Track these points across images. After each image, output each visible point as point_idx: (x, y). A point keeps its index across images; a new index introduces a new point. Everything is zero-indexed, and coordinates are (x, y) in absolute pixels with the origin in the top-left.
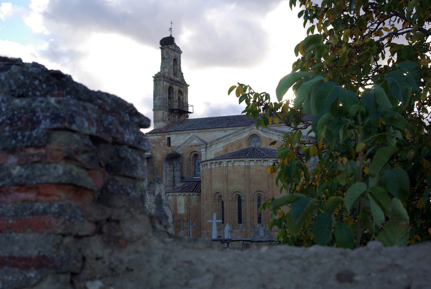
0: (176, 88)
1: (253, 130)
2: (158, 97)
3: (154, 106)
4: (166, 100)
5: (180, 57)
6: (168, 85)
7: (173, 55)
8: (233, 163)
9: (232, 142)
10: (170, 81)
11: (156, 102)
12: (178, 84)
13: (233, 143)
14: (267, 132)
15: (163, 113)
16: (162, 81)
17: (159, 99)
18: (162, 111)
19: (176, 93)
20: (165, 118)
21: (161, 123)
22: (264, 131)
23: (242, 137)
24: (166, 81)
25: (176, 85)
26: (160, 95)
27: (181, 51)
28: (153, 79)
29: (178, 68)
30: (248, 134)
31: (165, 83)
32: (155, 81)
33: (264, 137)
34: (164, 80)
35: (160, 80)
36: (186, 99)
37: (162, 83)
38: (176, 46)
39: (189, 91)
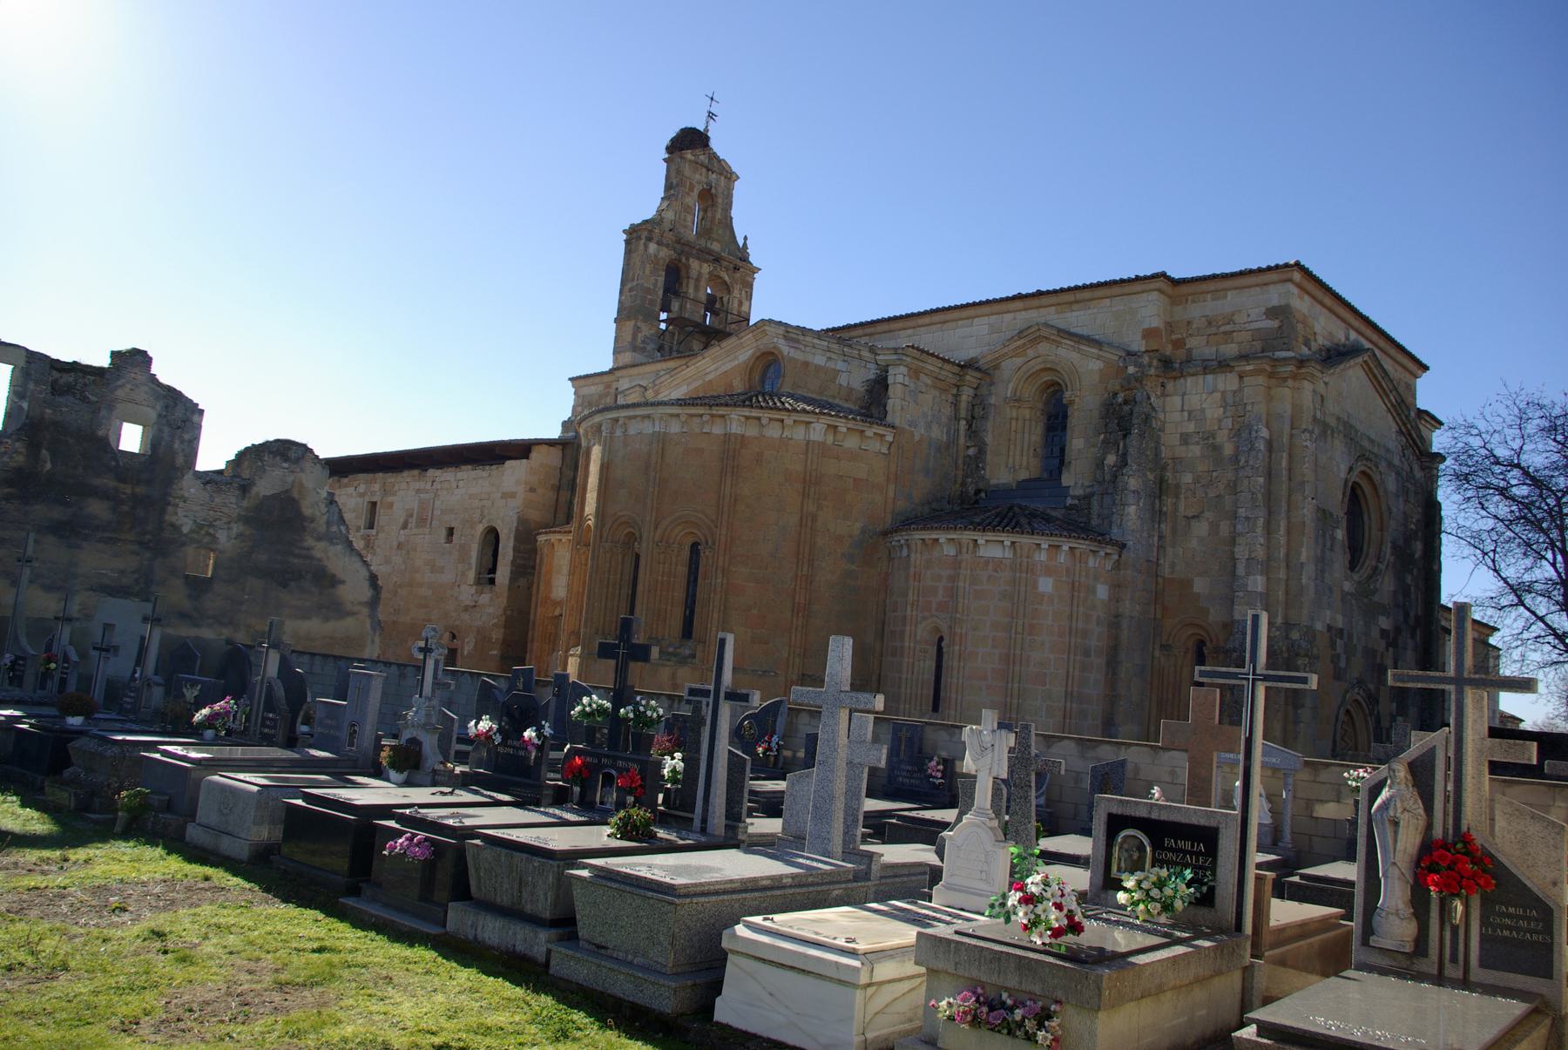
0: (698, 267)
6: (665, 253)
7: (699, 178)
14: (798, 341)
15: (637, 329)
18: (632, 323)
22: (792, 340)
24: (658, 243)
27: (732, 173)
29: (718, 216)
31: (652, 247)
32: (627, 242)
34: (649, 239)
35: (639, 238)
36: (741, 304)
37: (642, 247)
39: (756, 285)
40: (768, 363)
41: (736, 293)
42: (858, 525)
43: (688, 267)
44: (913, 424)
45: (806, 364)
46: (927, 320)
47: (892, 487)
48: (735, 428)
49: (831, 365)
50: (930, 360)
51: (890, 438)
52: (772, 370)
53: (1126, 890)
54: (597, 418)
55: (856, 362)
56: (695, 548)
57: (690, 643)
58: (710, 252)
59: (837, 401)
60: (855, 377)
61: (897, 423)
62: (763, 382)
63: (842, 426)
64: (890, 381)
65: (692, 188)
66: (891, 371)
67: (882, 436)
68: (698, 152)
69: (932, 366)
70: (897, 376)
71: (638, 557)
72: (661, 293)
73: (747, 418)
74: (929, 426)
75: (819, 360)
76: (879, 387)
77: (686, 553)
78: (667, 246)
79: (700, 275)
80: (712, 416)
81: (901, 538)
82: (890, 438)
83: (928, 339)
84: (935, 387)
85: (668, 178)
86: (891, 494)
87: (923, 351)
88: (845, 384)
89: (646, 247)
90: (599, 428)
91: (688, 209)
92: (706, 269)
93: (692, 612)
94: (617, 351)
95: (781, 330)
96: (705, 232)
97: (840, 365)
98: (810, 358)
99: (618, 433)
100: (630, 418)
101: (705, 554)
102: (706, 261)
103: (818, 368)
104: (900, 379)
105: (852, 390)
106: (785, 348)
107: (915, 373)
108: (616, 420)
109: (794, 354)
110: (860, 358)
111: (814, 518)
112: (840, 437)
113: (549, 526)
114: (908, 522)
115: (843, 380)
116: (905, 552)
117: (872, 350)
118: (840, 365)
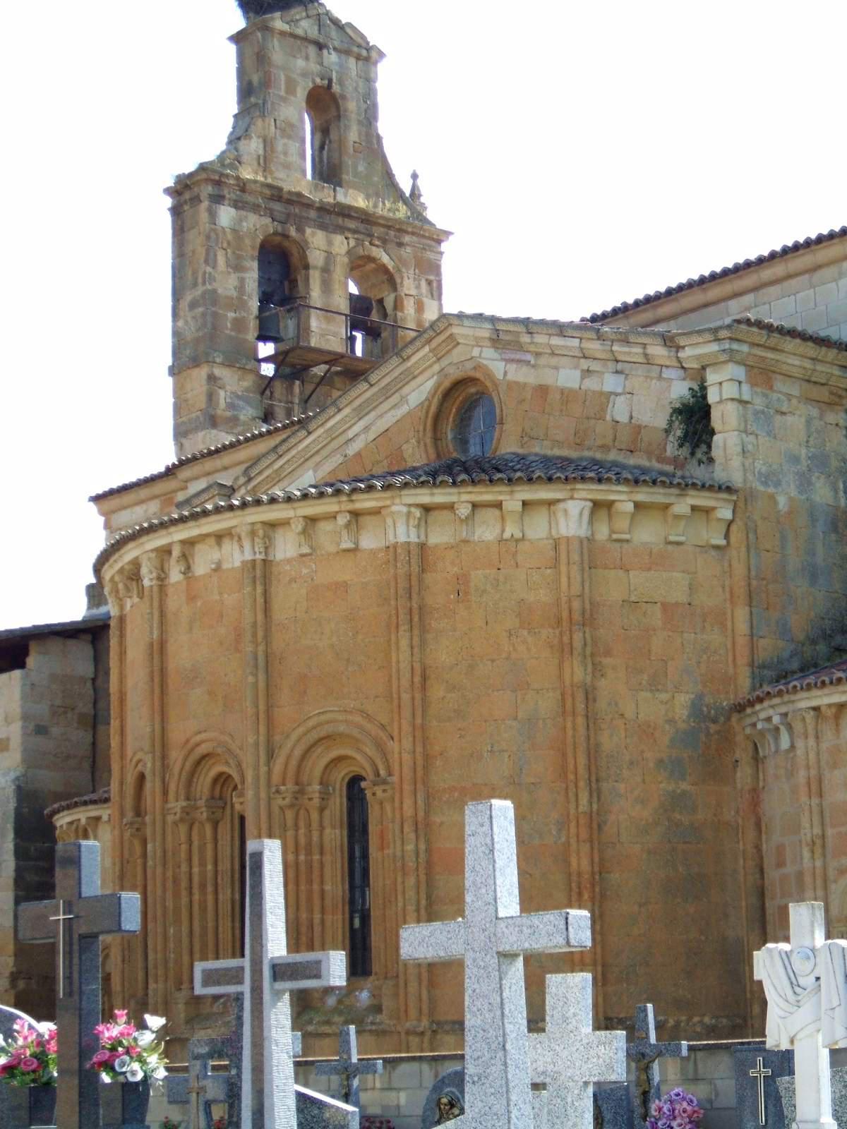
0: (322, 246)
1: (457, 355)
2: (188, 297)
3: (177, 352)
4: (240, 304)
5: (369, 80)
6: (257, 225)
8: (185, 558)
9: (352, 450)
10: (277, 207)
11: (180, 323)
12: (352, 224)
13: (359, 455)
14: (520, 347)
16: (205, 204)
17: (193, 305)
18: (203, 372)
19: (326, 270)
20: (231, 406)
21: (201, 434)
23: (404, 409)
24: (236, 205)
25: (323, 227)
26: (195, 285)
27: (369, 49)
28: (168, 202)
29: (353, 135)
30: (430, 384)
31: (226, 215)
32: (176, 211)
33: (512, 386)
34: (218, 199)
35: (196, 200)
36: (420, 307)
37: (204, 216)
38: (335, 22)
40: (465, 401)
41: (409, 285)
42: (683, 701)
43: (303, 248)
44: (769, 478)
45: (543, 390)
46: (778, 269)
47: (742, 614)
48: (404, 533)
49: (591, 384)
50: (791, 344)
51: (726, 514)
52: (479, 413)
53: (267, 360)
54: (130, 553)
55: (641, 371)
56: (354, 783)
57: (370, 982)
58: (345, 212)
59: (612, 456)
60: (647, 401)
61: (737, 479)
62: (463, 442)
63: (623, 498)
64: (712, 397)
65: (291, 89)
66: (712, 377)
67: (707, 511)
68: (297, 12)
69: (794, 357)
70: (724, 388)
71: (242, 819)
72: (254, 304)
73: (427, 509)
74: (805, 483)
75: (568, 377)
76: (695, 419)
77: (338, 803)
78: (255, 208)
79: (329, 256)
80: (356, 514)
81: (771, 712)
82: (726, 514)
83: (781, 307)
84: (809, 400)
85: (242, 72)
86: (742, 627)
87: (769, 328)
88: (623, 418)
89: (213, 215)
90: (133, 575)
91: (290, 131)
92: (340, 245)
93: (365, 919)
94: (181, 433)
95: (485, 332)
96: (329, 172)
97: (610, 383)
98: (547, 377)
99: (175, 576)
100: (189, 543)
101: (374, 794)
102: (340, 229)
103: (567, 396)
104: (730, 390)
105: (638, 429)
106: (497, 366)
107: (761, 374)
108: (166, 551)
109: (518, 374)
110: (648, 361)
111: (590, 695)
112: (622, 524)
113: (70, 799)
114: (781, 675)
115: (619, 410)
116: (785, 742)
117: (668, 341)
118: (610, 383)
